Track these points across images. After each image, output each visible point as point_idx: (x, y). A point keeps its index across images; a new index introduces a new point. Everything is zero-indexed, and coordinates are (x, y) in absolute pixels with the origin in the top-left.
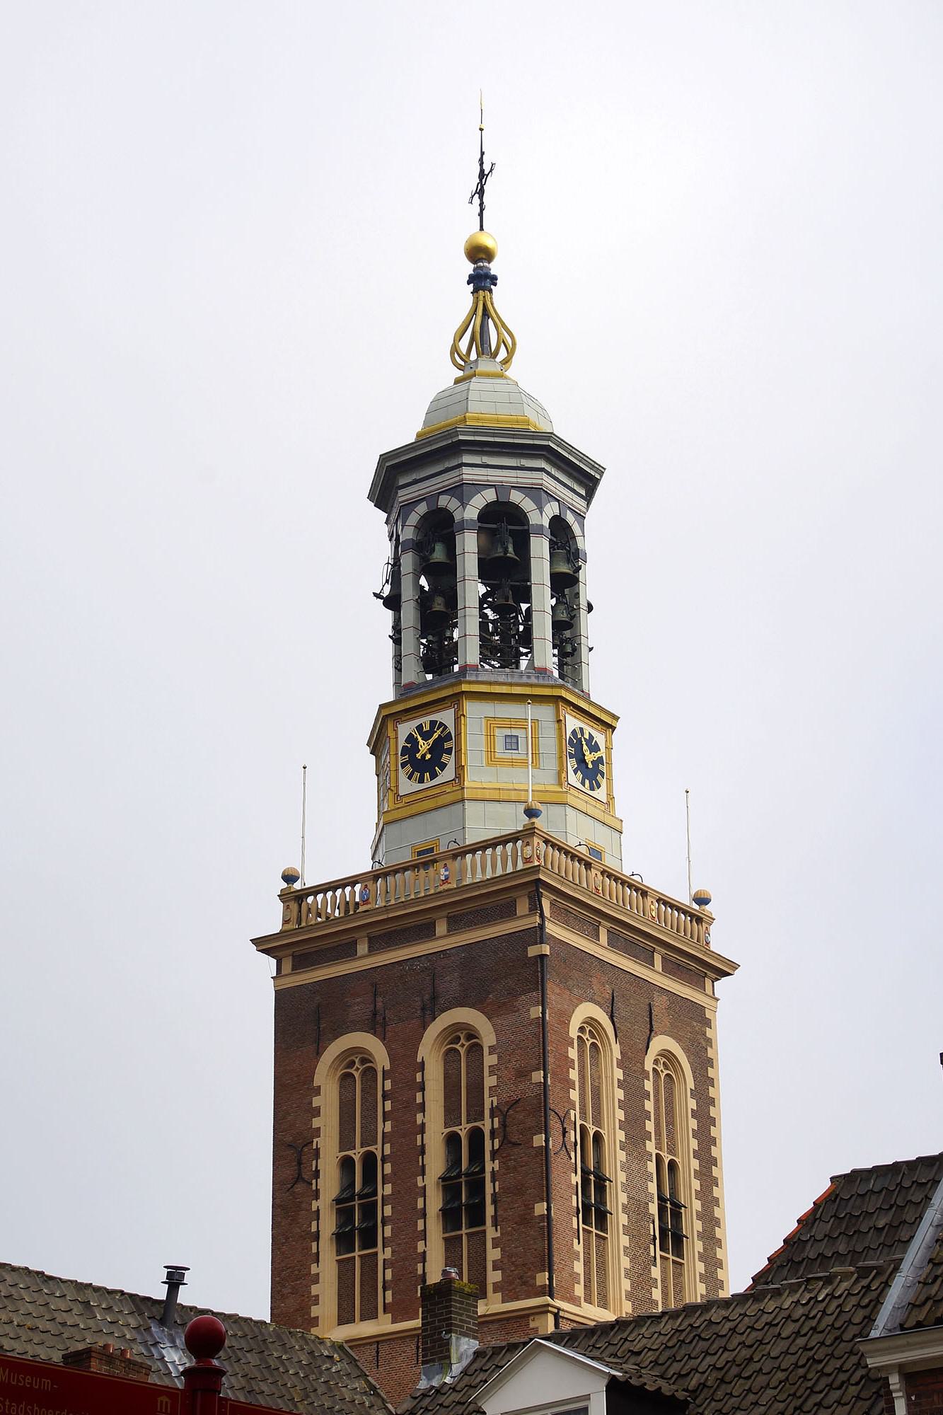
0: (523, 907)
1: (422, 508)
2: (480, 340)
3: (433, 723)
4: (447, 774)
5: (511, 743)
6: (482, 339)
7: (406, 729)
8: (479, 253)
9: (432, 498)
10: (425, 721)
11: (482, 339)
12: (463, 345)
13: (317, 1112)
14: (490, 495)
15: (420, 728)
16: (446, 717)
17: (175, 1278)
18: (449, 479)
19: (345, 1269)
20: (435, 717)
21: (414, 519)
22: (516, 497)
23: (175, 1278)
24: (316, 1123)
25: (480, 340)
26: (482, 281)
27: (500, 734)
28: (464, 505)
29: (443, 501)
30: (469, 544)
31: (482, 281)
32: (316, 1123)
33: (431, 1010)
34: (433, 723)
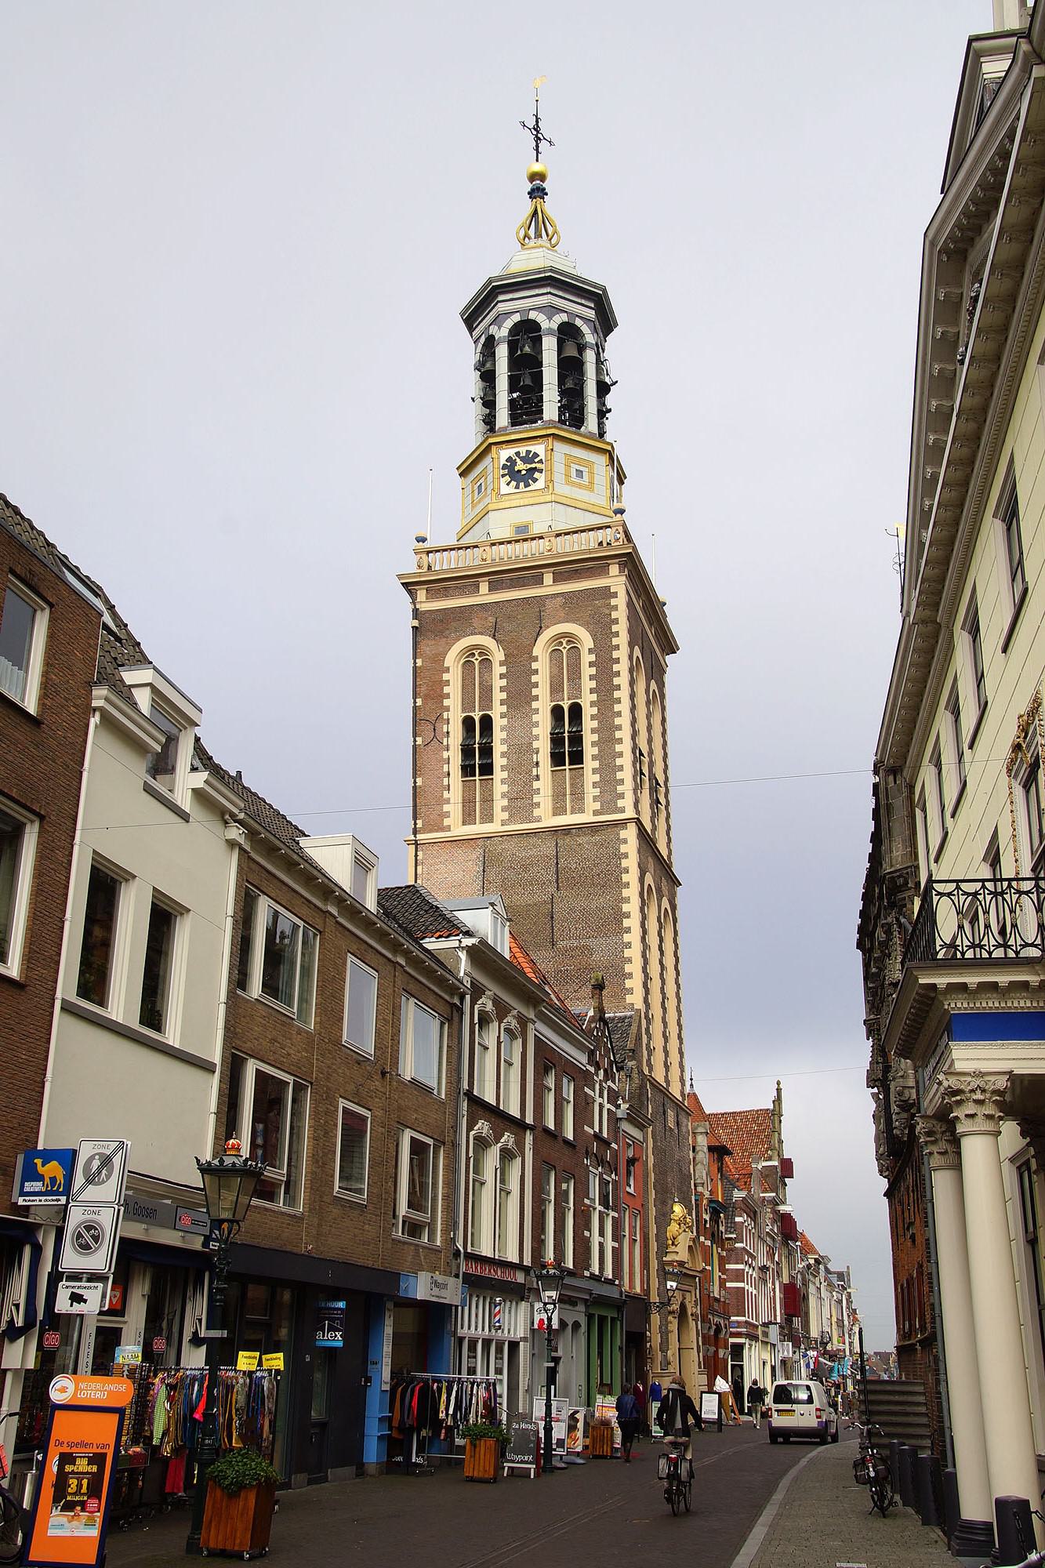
1: (517, 318)
3: (528, 452)
5: (580, 473)
7: (505, 453)
10: (523, 449)
14: (564, 317)
15: (518, 454)
16: (539, 449)
19: (468, 788)
21: (509, 323)
22: (578, 322)
26: (538, 193)
27: (575, 467)
28: (550, 319)
29: (533, 315)
30: (549, 345)
31: (538, 193)
34: (528, 452)
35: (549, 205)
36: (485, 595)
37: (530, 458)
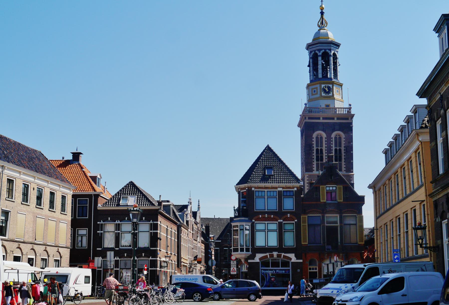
0: (350, 119)
1: (323, 51)
2: (322, 23)
4: (331, 94)
6: (322, 23)
8: (322, 9)
9: (325, 50)
11: (322, 23)
12: (319, 24)
13: (313, 141)
17: (63, 158)
18: (329, 48)
20: (329, 85)
21: (322, 52)
23: (63, 158)
24: (313, 143)
25: (322, 23)
26: (322, 13)
29: (327, 51)
31: (322, 13)
32: (313, 143)
33: (334, 130)
35: (325, 17)
36: (321, 121)
37: (329, 88)
